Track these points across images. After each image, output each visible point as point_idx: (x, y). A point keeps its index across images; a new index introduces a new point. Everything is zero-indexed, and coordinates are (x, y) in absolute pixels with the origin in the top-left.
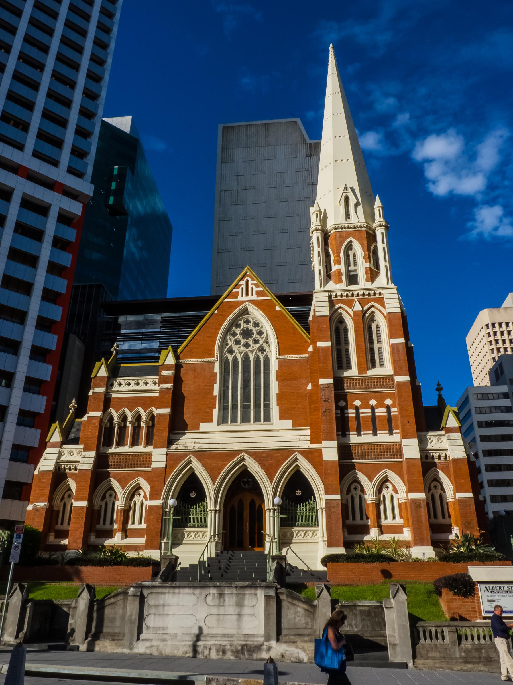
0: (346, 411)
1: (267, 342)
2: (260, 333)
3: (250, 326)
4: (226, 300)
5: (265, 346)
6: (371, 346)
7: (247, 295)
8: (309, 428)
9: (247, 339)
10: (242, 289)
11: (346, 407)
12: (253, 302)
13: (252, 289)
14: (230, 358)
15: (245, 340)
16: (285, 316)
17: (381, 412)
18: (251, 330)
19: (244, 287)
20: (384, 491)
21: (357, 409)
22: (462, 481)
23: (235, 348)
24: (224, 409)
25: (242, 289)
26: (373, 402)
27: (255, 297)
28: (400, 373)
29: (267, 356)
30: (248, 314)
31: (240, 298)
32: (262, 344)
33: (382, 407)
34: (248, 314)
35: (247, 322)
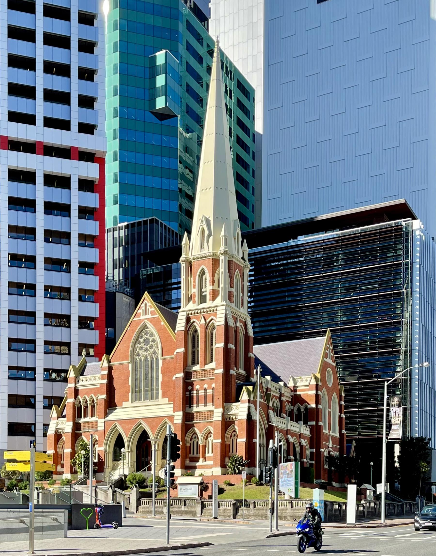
0: (192, 392)
1: (158, 347)
2: (154, 341)
3: (148, 337)
4: (134, 319)
5: (156, 350)
6: (211, 347)
7: (146, 315)
8: (172, 403)
9: (147, 346)
10: (143, 310)
11: (192, 390)
12: (148, 319)
13: (149, 309)
14: (138, 359)
15: (146, 347)
16: (166, 328)
17: (210, 392)
18: (149, 339)
19: (144, 308)
20: (209, 439)
21: (197, 390)
22: (242, 432)
23: (141, 352)
24: (135, 392)
25: (143, 310)
26: (206, 386)
27: (149, 316)
28: (218, 367)
29: (157, 357)
30: (148, 328)
31: (142, 317)
32: (155, 349)
33: (210, 389)
34: (148, 328)
35: (146, 334)
